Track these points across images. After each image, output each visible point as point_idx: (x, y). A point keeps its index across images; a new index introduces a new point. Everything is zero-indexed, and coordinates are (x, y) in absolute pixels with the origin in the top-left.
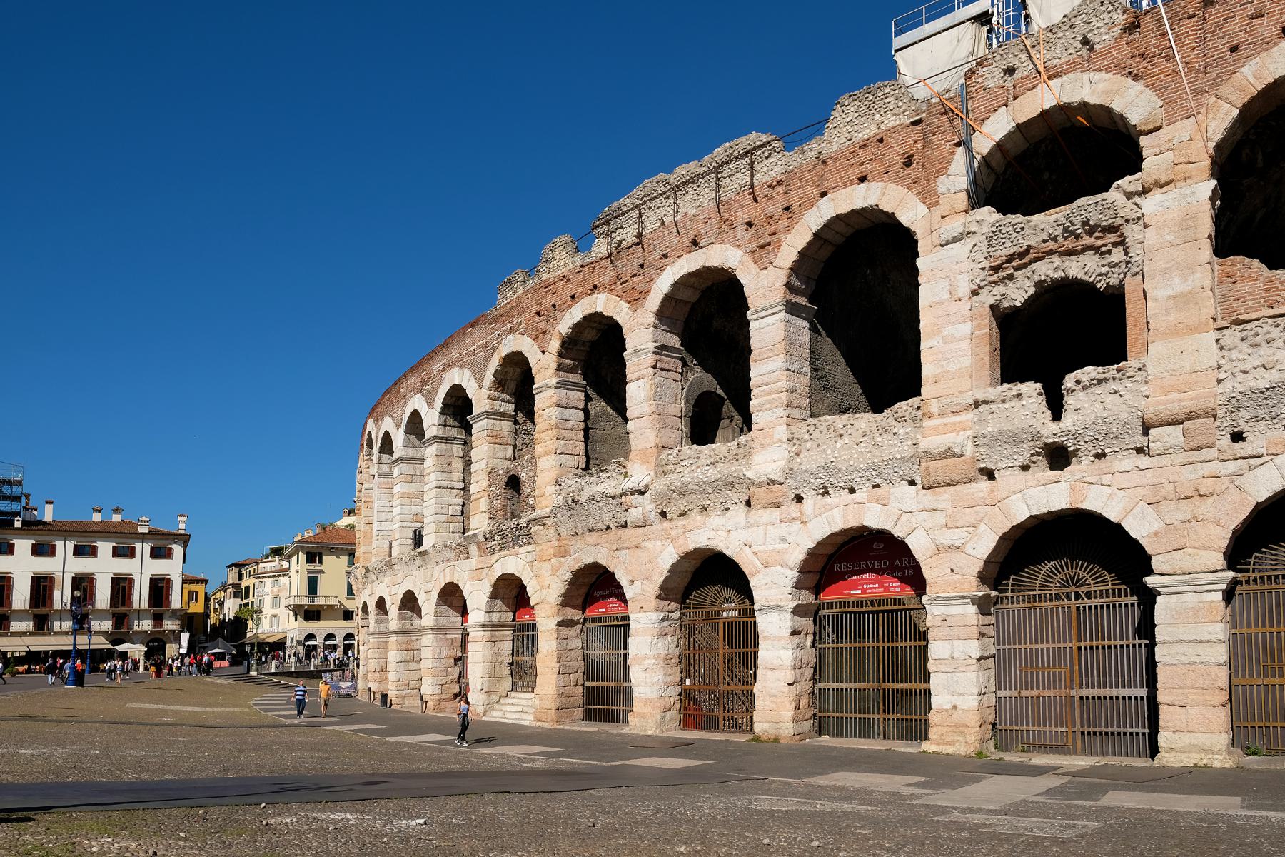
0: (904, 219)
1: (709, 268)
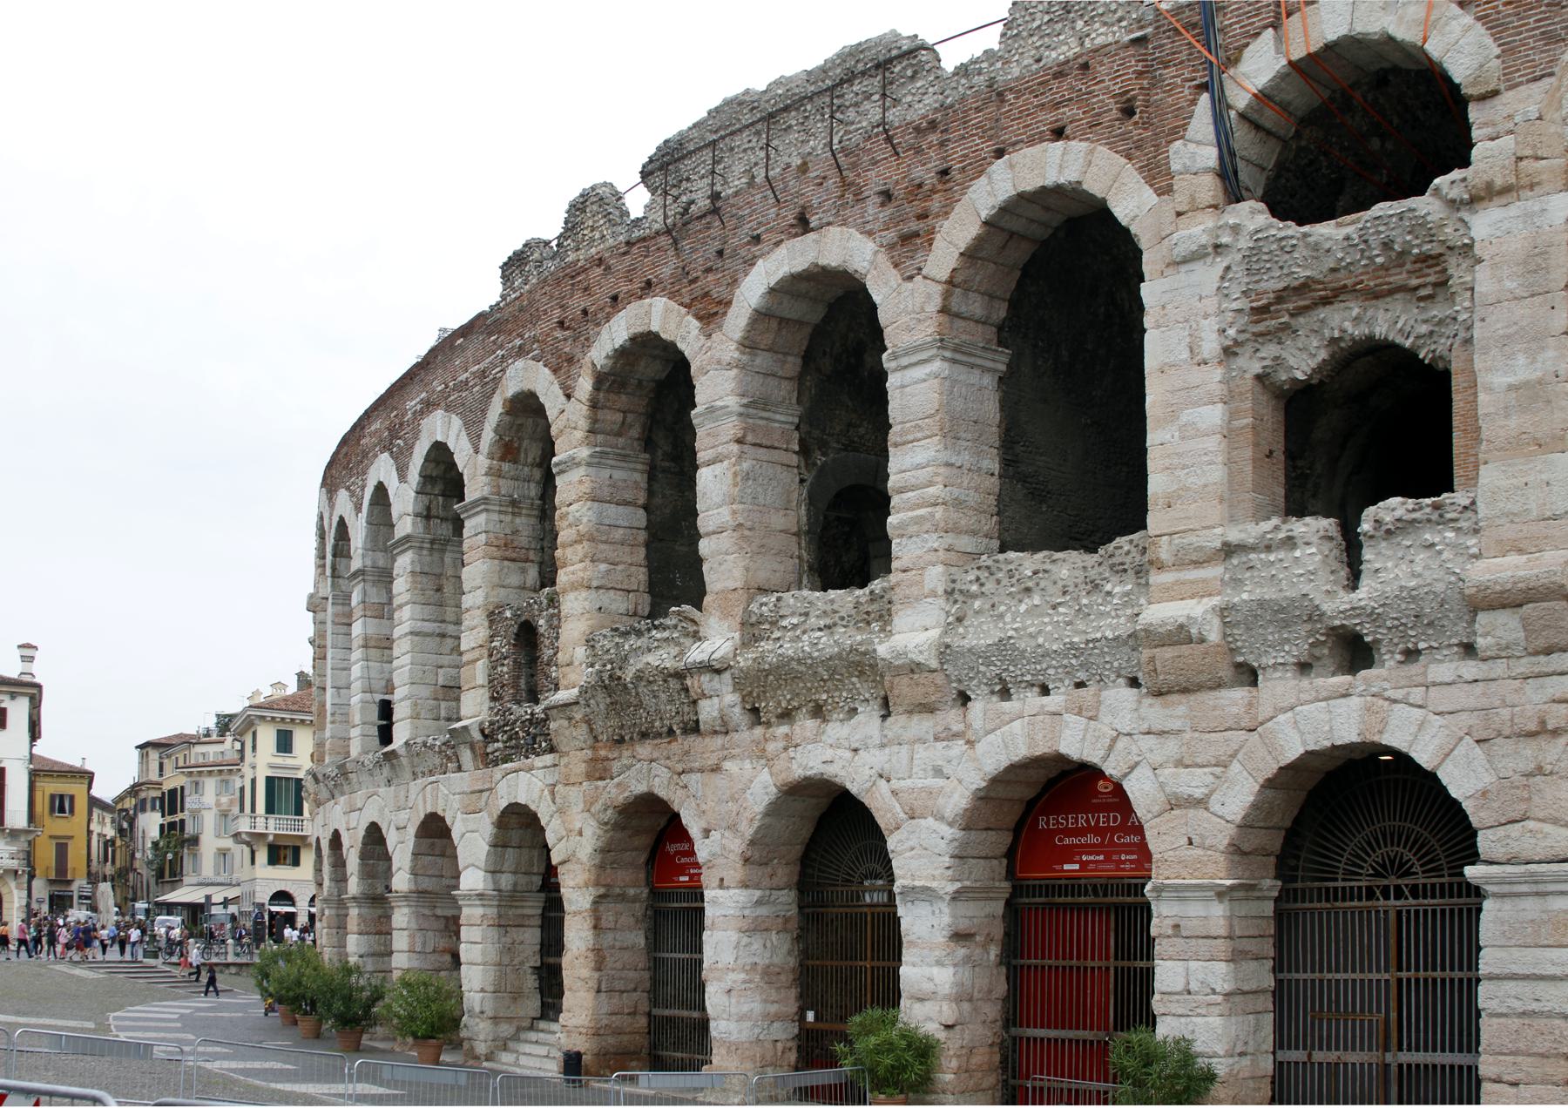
0: (1122, 211)
1: (824, 268)
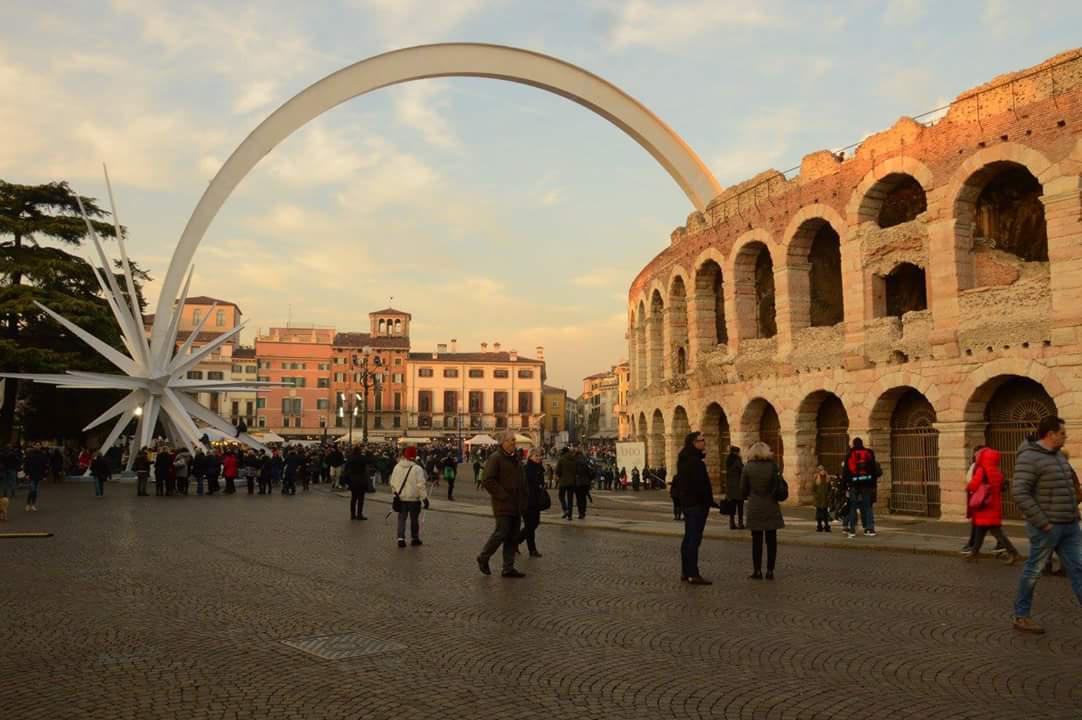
0: (834, 226)
